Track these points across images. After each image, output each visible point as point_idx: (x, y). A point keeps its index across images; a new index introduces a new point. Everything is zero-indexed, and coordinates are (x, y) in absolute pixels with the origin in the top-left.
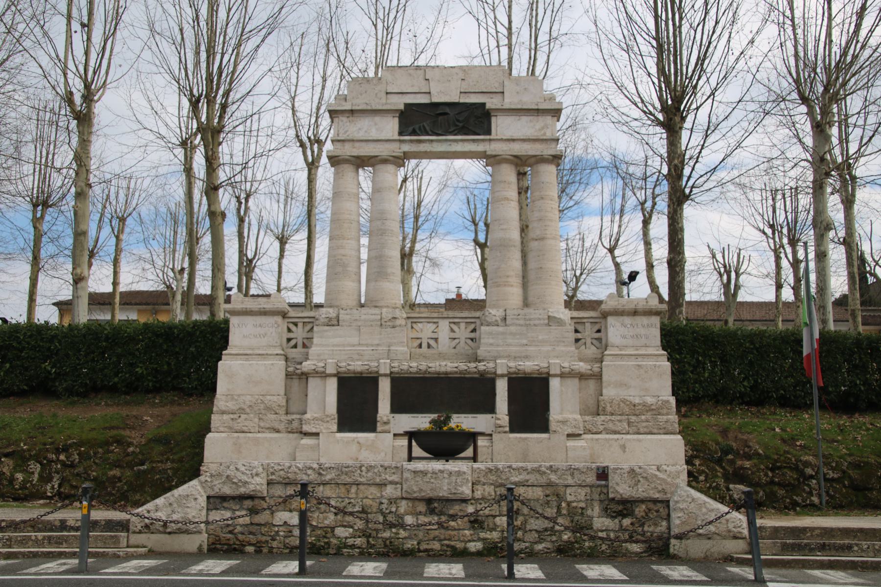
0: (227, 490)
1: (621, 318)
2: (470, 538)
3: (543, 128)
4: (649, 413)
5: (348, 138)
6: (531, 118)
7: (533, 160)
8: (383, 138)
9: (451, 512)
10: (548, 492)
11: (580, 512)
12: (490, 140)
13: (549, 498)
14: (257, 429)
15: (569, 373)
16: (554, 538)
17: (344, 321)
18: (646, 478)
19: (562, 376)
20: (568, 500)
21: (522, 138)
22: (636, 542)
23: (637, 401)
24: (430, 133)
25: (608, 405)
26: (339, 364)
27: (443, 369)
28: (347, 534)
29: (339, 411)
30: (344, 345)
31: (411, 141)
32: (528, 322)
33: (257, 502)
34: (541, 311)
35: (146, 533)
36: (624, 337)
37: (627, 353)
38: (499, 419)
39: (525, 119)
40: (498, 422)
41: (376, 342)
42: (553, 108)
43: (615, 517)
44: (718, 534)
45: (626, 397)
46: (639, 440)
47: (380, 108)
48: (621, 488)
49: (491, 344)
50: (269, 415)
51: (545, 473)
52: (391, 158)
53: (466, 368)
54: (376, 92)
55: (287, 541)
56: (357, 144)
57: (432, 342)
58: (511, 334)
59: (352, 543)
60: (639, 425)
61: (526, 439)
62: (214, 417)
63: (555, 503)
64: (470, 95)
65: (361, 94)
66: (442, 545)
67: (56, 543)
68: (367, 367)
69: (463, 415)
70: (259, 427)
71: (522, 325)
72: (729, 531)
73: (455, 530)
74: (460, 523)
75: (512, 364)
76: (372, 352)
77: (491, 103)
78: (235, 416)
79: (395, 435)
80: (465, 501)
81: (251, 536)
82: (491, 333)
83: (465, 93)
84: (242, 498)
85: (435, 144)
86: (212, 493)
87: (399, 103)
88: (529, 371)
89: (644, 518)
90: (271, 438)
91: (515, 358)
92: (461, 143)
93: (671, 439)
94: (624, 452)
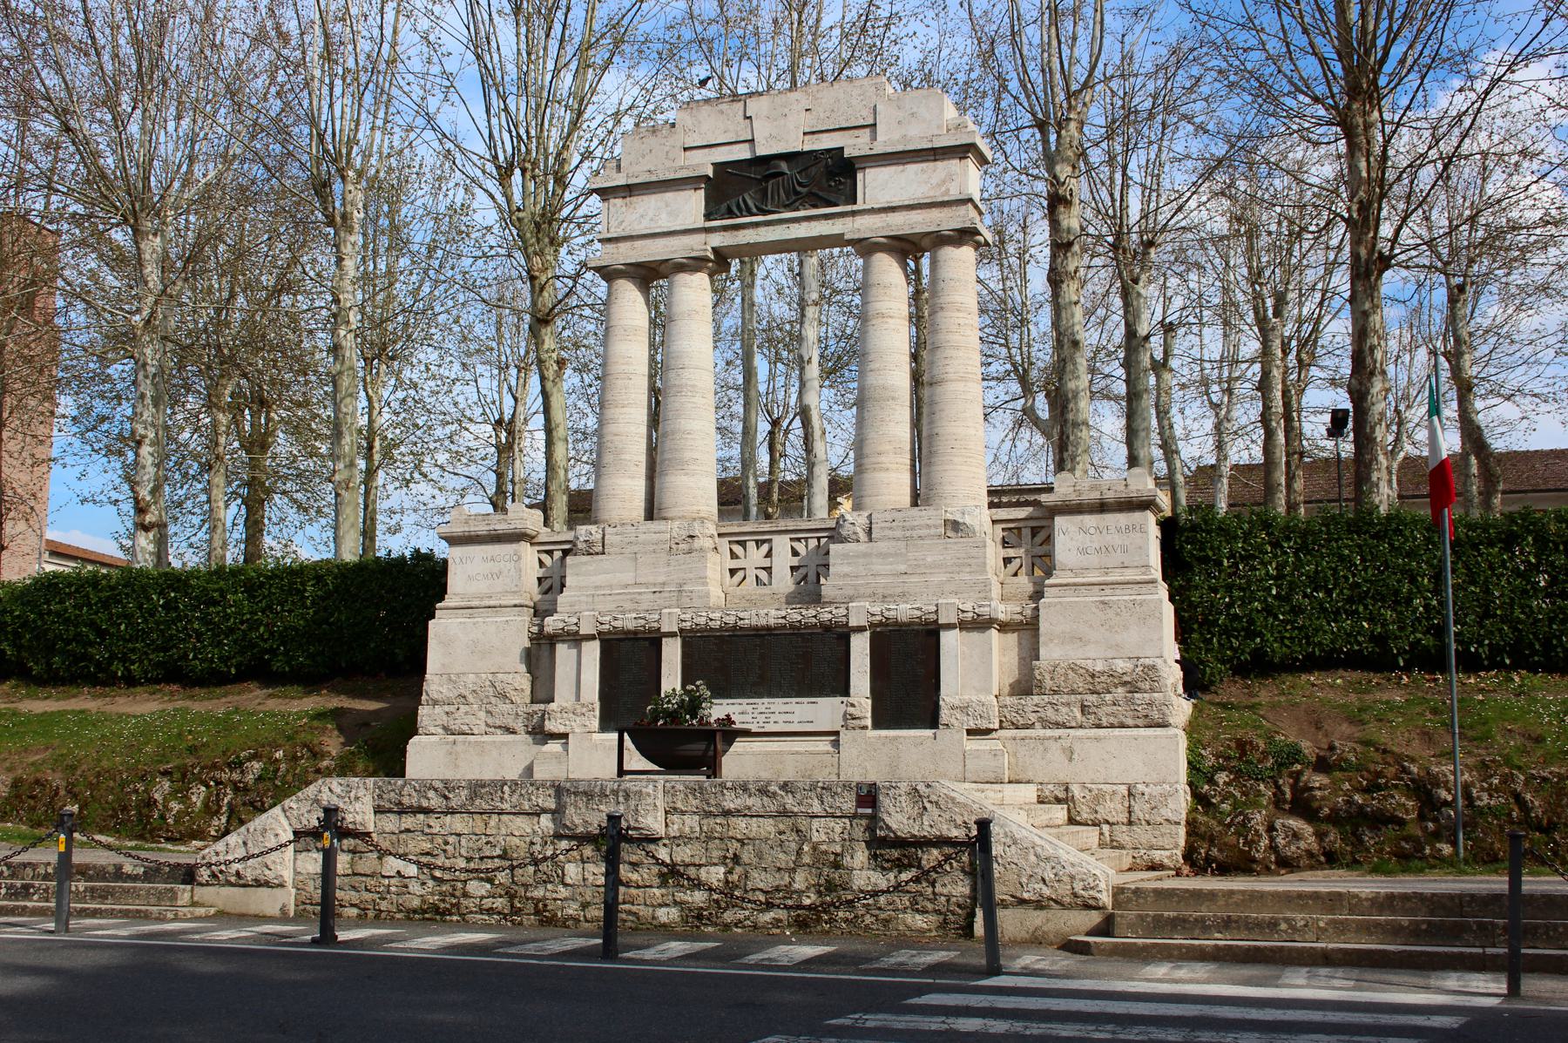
2: (660, 901)
3: (944, 182)
4: (1120, 690)
5: (623, 234)
6: (924, 165)
8: (678, 228)
10: (782, 827)
11: (832, 858)
13: (783, 837)
14: (483, 727)
15: (974, 621)
17: (612, 545)
18: (937, 803)
19: (964, 626)
20: (814, 839)
21: (906, 203)
22: (924, 912)
23: (1099, 666)
24: (754, 210)
25: (1047, 677)
26: (600, 619)
27: (763, 622)
30: (611, 587)
31: (725, 228)
32: (908, 534)
35: (213, 885)
36: (1084, 551)
38: (853, 705)
40: (851, 710)
41: (661, 579)
42: (958, 143)
43: (890, 870)
44: (1056, 901)
45: (1078, 662)
46: (1097, 739)
47: (672, 176)
48: (898, 819)
49: (846, 575)
51: (775, 794)
52: (691, 261)
53: (800, 618)
54: (667, 149)
56: (638, 243)
57: (763, 575)
58: (880, 555)
59: (490, 905)
60: (1101, 712)
61: (896, 738)
62: (423, 711)
63: (793, 845)
64: (821, 135)
65: (643, 156)
67: (100, 897)
68: (643, 622)
69: (794, 700)
70: (487, 725)
71: (899, 539)
72: (1075, 895)
73: (638, 887)
74: (645, 876)
75: (876, 609)
76: (652, 596)
77: (855, 145)
78: (452, 708)
81: (353, 893)
82: (846, 556)
83: (813, 133)
85: (762, 230)
87: (704, 163)
88: (904, 620)
90: (503, 743)
91: (884, 597)
92: (805, 224)
93: (1156, 737)
94: (1071, 760)
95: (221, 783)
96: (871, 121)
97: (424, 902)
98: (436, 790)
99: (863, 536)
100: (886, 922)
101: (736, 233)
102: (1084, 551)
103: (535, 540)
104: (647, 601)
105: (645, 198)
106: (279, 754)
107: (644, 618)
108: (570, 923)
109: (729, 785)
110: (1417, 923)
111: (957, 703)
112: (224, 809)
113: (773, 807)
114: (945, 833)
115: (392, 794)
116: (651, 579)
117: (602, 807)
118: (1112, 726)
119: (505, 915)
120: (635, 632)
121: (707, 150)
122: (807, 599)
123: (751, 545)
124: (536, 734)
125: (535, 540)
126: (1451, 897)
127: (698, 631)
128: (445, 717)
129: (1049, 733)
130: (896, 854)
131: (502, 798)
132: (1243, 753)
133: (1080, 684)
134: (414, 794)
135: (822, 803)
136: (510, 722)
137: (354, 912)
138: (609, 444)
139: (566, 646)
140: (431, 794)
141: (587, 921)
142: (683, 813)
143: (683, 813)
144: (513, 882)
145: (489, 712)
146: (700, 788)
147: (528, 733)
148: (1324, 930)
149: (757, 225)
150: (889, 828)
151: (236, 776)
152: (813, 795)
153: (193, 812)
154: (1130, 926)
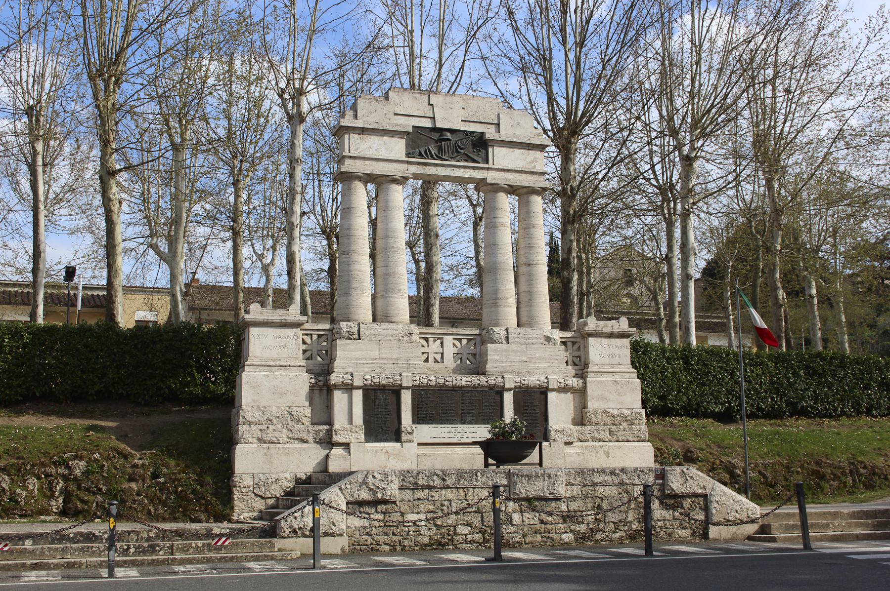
0: (365, 495)
1: (599, 339)
3: (533, 161)
4: (625, 424)
5: (360, 155)
6: (523, 151)
7: (525, 190)
8: (393, 159)
9: (549, 509)
12: (488, 169)
13: (621, 495)
14: (286, 439)
15: (564, 388)
16: (626, 528)
22: (685, 528)
23: (616, 412)
27: (459, 383)
28: (467, 532)
29: (365, 422)
31: (419, 164)
32: (527, 341)
33: (389, 506)
34: (538, 331)
35: (292, 537)
37: (605, 370)
39: (518, 152)
41: (395, 356)
47: (391, 129)
49: (496, 361)
50: (296, 426)
51: (618, 474)
54: (385, 112)
55: (417, 540)
56: (367, 162)
62: (242, 428)
64: (469, 123)
65: (371, 113)
66: (542, 537)
68: (391, 380)
69: (477, 426)
70: (288, 437)
72: (749, 517)
73: (552, 524)
75: (518, 380)
77: (490, 133)
79: (419, 444)
80: (558, 499)
81: (386, 537)
82: (496, 350)
83: (465, 121)
84: (375, 503)
85: (440, 168)
86: (351, 499)
87: (408, 124)
89: (689, 509)
92: (462, 170)
94: (608, 457)
95: (51, 476)
96: (496, 122)
97: (431, 539)
98: (438, 476)
99: (504, 342)
100: (670, 534)
101: (424, 167)
102: (602, 356)
103: (303, 327)
104: (389, 368)
105: (372, 137)
106: (97, 455)
107: (392, 378)
108: (516, 545)
109: (596, 470)
110: (874, 522)
111: (558, 429)
112: (57, 494)
113: (617, 481)
114: (696, 491)
115: (411, 478)
116: (389, 356)
117: (536, 483)
118: (623, 441)
119: (480, 544)
120: (384, 386)
121: (407, 118)
122: (464, 371)
123: (431, 340)
124: (321, 443)
125: (303, 327)
126: (872, 511)
127: (422, 387)
128: (259, 433)
129: (597, 444)
130: (672, 502)
131: (476, 479)
132: (662, 454)
133: (608, 421)
134: (425, 478)
135: (639, 478)
136: (304, 436)
137: (387, 548)
138: (356, 276)
139: (340, 392)
140: (435, 478)
141: (526, 543)
142: (573, 485)
143: (573, 485)
144: (483, 525)
145: (288, 430)
146: (582, 471)
147: (316, 442)
148: (844, 526)
149: (436, 165)
150: (672, 489)
151: (62, 470)
152: (635, 474)
153: (35, 496)
154: (777, 529)
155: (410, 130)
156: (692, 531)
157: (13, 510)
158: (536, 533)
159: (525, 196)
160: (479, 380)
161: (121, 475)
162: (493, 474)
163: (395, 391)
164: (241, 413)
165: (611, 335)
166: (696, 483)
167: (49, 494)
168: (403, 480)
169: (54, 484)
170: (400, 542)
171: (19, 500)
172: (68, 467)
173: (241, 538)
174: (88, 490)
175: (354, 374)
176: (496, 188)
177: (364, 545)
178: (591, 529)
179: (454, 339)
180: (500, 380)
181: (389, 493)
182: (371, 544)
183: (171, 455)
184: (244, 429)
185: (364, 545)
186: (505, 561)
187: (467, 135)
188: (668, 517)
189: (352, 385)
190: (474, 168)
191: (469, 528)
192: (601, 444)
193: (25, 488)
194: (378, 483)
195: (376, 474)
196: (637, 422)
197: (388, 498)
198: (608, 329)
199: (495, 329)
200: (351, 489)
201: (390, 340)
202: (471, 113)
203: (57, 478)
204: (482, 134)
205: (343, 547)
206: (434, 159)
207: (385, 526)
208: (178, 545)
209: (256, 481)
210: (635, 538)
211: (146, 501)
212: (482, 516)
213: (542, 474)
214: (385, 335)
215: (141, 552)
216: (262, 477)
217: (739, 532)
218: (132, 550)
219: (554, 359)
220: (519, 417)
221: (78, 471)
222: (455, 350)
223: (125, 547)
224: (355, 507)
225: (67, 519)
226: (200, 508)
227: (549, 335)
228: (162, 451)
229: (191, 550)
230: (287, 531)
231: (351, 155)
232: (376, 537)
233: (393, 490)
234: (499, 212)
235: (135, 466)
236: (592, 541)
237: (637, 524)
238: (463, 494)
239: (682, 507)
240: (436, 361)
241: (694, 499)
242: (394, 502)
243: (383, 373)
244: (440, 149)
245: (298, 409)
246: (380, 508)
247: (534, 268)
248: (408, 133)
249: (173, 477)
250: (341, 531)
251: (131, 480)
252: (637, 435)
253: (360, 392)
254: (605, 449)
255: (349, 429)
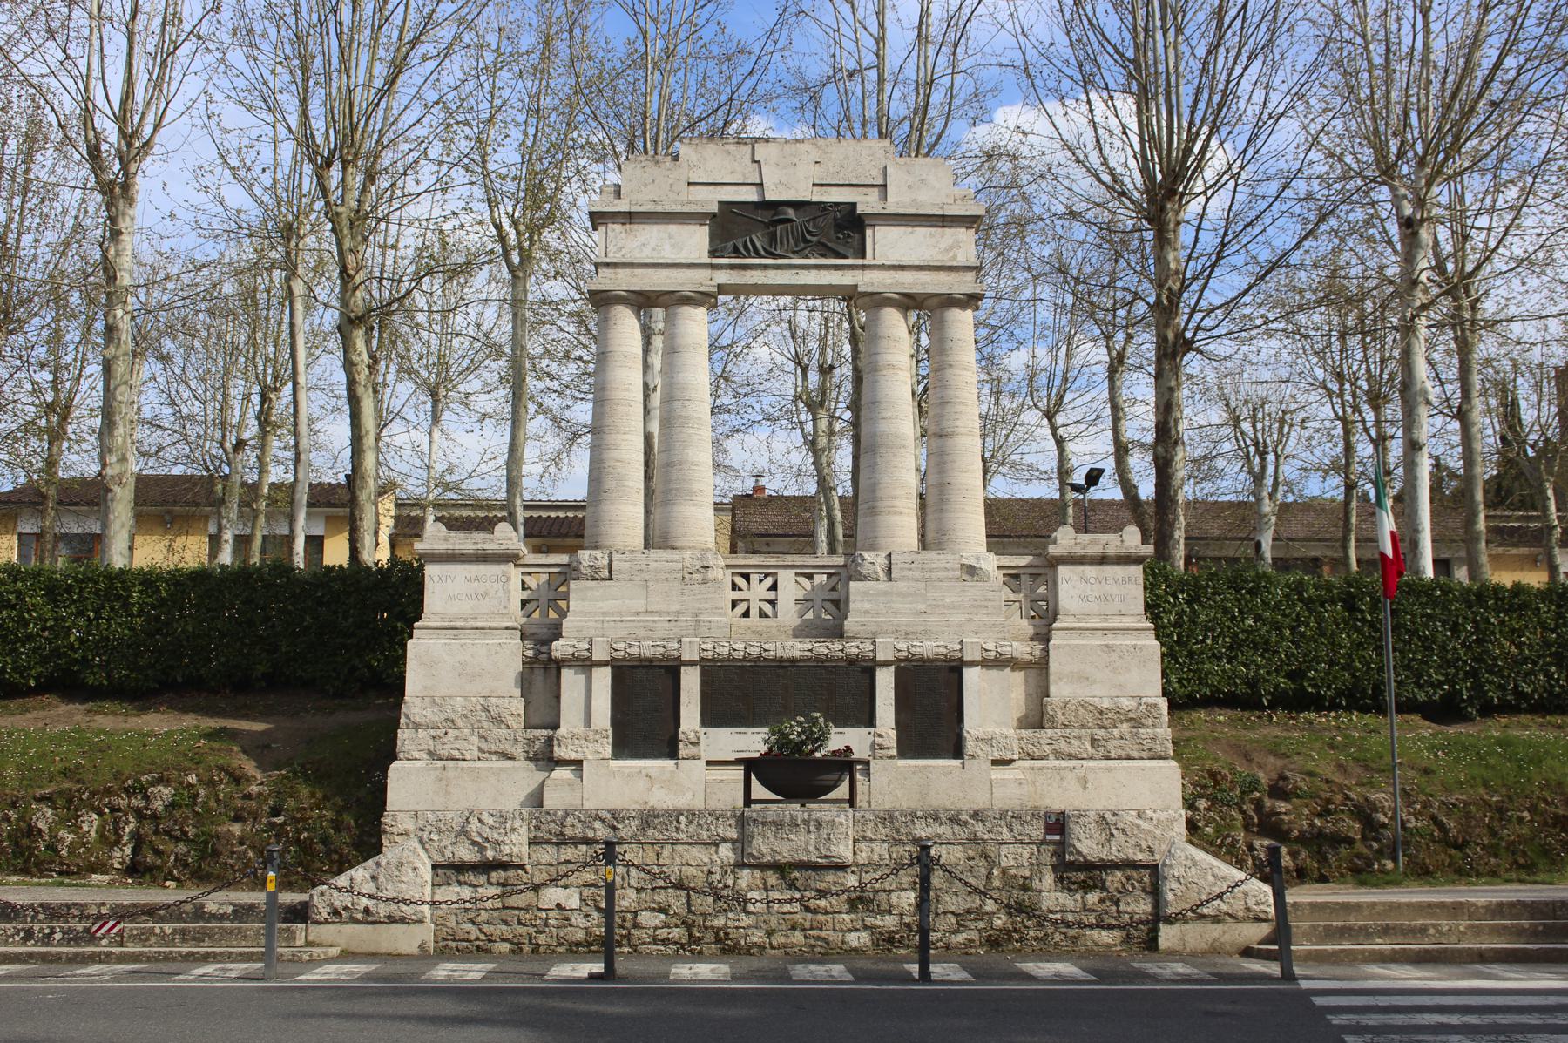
0: (465, 854)
1: (1080, 568)
2: (850, 926)
3: (951, 248)
4: (1125, 725)
5: (624, 260)
7: (935, 301)
8: (683, 261)
9: (822, 886)
10: (971, 853)
11: (1021, 882)
12: (864, 267)
13: (972, 863)
14: (476, 753)
16: (981, 925)
17: (620, 572)
18: (1123, 830)
19: (986, 664)
20: (1003, 864)
21: (917, 263)
22: (1110, 927)
23: (1106, 704)
24: (763, 253)
25: (1059, 712)
26: (614, 646)
27: (788, 654)
28: (657, 923)
29: (616, 723)
30: (620, 613)
31: (732, 267)
32: (927, 575)
33: (512, 873)
34: (949, 557)
35: (333, 923)
36: (1085, 599)
37: (1088, 625)
38: (880, 736)
39: (922, 232)
40: (878, 740)
41: (675, 608)
42: (968, 213)
43: (1076, 891)
44: (1231, 916)
45: (1087, 699)
46: (1108, 769)
47: (679, 209)
48: (1087, 844)
49: (867, 612)
50: (496, 731)
51: (966, 823)
52: (698, 296)
53: (826, 651)
54: (671, 181)
55: (562, 934)
56: (638, 271)
57: (767, 608)
58: (900, 594)
59: (665, 935)
60: (1110, 745)
61: (925, 767)
62: (403, 735)
63: (983, 870)
64: (829, 189)
65: (646, 185)
66: (806, 937)
67: (194, 939)
68: (662, 650)
70: (480, 750)
71: (918, 580)
72: (1248, 910)
73: (826, 913)
74: (834, 902)
75: (902, 645)
76: (667, 624)
77: (867, 203)
78: (439, 733)
79: (708, 763)
80: (840, 867)
81: (504, 927)
82: (866, 593)
83: (822, 185)
84: (485, 867)
86: (440, 859)
87: (709, 200)
88: (930, 656)
89: (1120, 892)
90: (501, 769)
91: (907, 634)
92: (814, 272)
93: (1161, 768)
94: (1085, 788)
95: (119, 810)
96: (880, 182)
97: (588, 934)
98: (603, 821)
99: (882, 576)
100: (1075, 939)
101: (743, 272)
102: (1085, 599)
103: (521, 562)
104: (662, 629)
105: (647, 227)
106: (192, 779)
107: (664, 647)
108: (754, 950)
109: (919, 814)
110: (1536, 926)
111: (981, 735)
112: (125, 839)
113: (963, 835)
114: (1131, 857)
115: (552, 825)
116: (664, 607)
117: (792, 836)
118: (1119, 758)
119: (683, 946)
120: (651, 660)
121: (711, 188)
122: (815, 632)
123: (754, 578)
124: (538, 760)
125: (521, 562)
126: (1546, 904)
127: (720, 661)
128: (431, 742)
129: (1063, 763)
130: (1082, 876)
131: (677, 829)
132: (1217, 783)
133: (1090, 720)
134: (579, 824)
135: (1011, 830)
136: (508, 747)
137: (506, 947)
138: (611, 470)
139: (572, 671)
140: (598, 824)
141: (772, 947)
142: (872, 841)
143: (872, 841)
144: (690, 911)
145: (481, 737)
146: (890, 817)
147: (528, 759)
148: (1464, 933)
149: (765, 267)
150: (1079, 853)
151: (137, 802)
152: (1003, 823)
153: (88, 842)
154: (1305, 935)
155: (715, 208)
156: (1124, 933)
157: (49, 863)
158: (793, 928)
159: (938, 311)
160: (827, 647)
161: (223, 810)
162: (710, 819)
163: (670, 670)
164: (404, 709)
165: (1103, 560)
166: (1133, 841)
167: (113, 838)
168: (537, 828)
169: (122, 824)
170: (530, 936)
171: (60, 848)
172: (146, 797)
173: (253, 922)
174: (168, 833)
175: (683, 640)
176: (876, 301)
177: (463, 940)
178: (908, 925)
179: (797, 574)
180: (868, 646)
181: (506, 849)
182: (477, 939)
183: (306, 778)
184: (406, 736)
185: (463, 940)
186: (622, 979)
187: (824, 209)
188: (1070, 904)
189: (589, 659)
190: (836, 267)
191: (663, 916)
192: (1073, 763)
193: (75, 829)
194: (487, 832)
195: (485, 817)
196: (1149, 722)
197: (505, 859)
198: (1095, 549)
199: (866, 555)
200: (440, 841)
201: (667, 579)
202: (831, 170)
203: (126, 815)
204: (853, 206)
205: (423, 943)
206: (761, 256)
207: (504, 907)
208: (131, 930)
209: (421, 823)
210: (999, 945)
211: (251, 854)
212: (688, 896)
213: (804, 821)
214: (656, 571)
215: (71, 939)
216: (431, 817)
217: (1226, 938)
218: (58, 936)
219: (981, 607)
220: (824, 716)
221: (160, 803)
222: (801, 595)
223: (47, 931)
224: (448, 873)
225: (130, 881)
226: (330, 867)
227: (973, 562)
228: (295, 772)
229: (153, 939)
230: (324, 913)
231: (608, 260)
232: (486, 928)
233: (516, 844)
234: (883, 343)
235: (248, 797)
236: (908, 947)
237: (1004, 918)
238: (652, 854)
239: (1104, 888)
240: (762, 614)
241: (1129, 872)
242: (522, 867)
243: (649, 638)
244: (772, 238)
245: (500, 702)
246: (495, 876)
247: (950, 442)
248: (714, 215)
249: (298, 815)
250: (420, 915)
251: (237, 819)
252: (1149, 746)
253: (607, 671)
254: (1081, 773)
255: (583, 736)
